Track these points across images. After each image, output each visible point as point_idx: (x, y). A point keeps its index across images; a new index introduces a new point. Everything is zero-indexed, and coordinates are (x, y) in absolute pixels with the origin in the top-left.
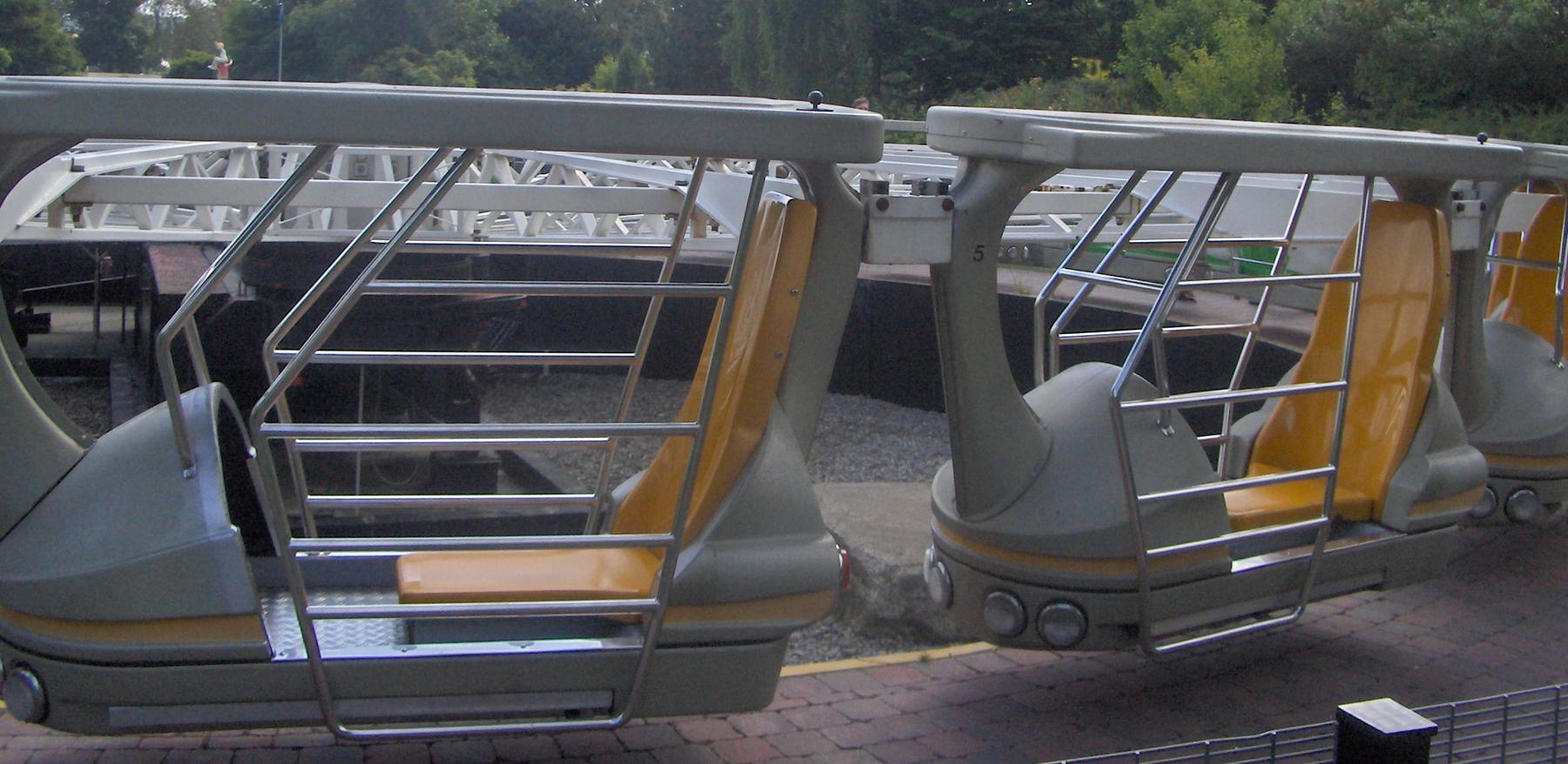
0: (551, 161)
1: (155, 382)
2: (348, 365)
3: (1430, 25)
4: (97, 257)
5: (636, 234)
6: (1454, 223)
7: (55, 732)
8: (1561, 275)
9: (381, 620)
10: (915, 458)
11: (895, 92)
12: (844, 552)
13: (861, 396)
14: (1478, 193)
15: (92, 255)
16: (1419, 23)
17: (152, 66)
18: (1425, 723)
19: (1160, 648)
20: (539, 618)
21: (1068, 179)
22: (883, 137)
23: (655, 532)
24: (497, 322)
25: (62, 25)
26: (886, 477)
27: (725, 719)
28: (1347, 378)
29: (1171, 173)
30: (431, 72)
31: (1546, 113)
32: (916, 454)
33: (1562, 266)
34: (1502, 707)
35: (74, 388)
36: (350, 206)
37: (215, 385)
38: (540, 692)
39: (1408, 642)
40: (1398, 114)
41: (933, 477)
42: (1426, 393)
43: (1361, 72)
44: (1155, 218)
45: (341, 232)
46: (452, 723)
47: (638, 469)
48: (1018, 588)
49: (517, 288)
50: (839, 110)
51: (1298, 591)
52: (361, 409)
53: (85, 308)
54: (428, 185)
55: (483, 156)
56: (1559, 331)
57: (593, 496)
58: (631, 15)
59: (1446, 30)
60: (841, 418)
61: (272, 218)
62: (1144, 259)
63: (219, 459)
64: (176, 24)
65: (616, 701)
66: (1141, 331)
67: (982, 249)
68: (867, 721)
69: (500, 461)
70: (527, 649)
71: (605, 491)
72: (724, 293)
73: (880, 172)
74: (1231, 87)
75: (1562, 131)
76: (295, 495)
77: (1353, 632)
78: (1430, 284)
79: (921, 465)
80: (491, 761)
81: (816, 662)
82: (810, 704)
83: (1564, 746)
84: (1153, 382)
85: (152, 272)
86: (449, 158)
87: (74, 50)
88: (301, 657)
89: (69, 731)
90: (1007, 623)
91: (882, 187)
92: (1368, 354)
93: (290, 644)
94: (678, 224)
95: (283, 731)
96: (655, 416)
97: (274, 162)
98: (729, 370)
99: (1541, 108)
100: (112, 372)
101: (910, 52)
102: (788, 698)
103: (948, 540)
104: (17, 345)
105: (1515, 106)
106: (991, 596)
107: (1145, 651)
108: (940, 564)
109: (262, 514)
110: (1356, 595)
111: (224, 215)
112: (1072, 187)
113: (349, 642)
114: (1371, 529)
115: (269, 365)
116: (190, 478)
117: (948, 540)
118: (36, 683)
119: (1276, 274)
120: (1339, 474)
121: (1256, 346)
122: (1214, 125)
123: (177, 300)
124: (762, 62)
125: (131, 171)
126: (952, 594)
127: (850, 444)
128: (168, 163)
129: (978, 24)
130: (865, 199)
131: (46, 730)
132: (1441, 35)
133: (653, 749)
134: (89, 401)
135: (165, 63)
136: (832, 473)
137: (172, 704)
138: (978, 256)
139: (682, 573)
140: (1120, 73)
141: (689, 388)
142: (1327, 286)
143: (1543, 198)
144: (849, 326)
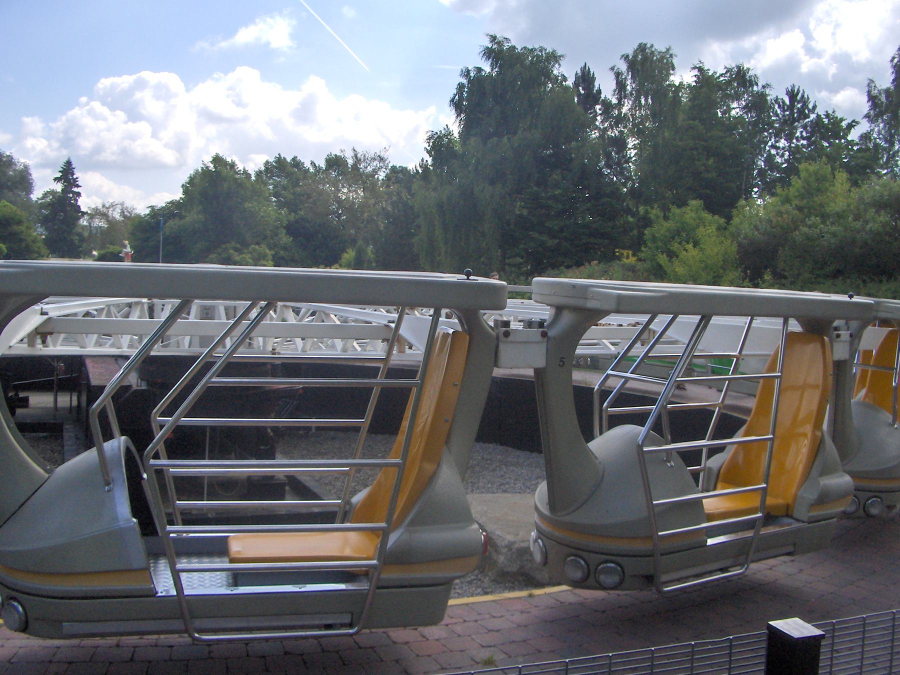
0: (316, 309)
1: (89, 436)
2: (200, 426)
3: (821, 231)
4: (55, 364)
5: (365, 351)
6: (835, 344)
7: (32, 637)
8: (896, 375)
9: (218, 573)
10: (525, 480)
11: (513, 269)
12: (484, 533)
13: (494, 444)
14: (848, 328)
15: (53, 363)
16: (814, 230)
17: (87, 254)
18: (818, 632)
19: (666, 589)
20: (309, 572)
21: (613, 320)
22: (507, 295)
23: (376, 522)
24: (285, 402)
25: (35, 231)
26: (509, 490)
27: (416, 629)
28: (773, 434)
29: (672, 316)
30: (247, 258)
31: (888, 281)
32: (526, 477)
33: (896, 369)
34: (862, 623)
35: (43, 439)
36: (201, 335)
37: (123, 438)
38: (310, 614)
39: (808, 586)
40: (803, 282)
41: (536, 490)
42: (818, 442)
43: (781, 258)
44: (662, 341)
45: (196, 350)
46: (259, 632)
47: (366, 486)
48: (584, 554)
49: (296, 382)
50: (481, 280)
51: (745, 556)
52: (207, 452)
53: (49, 393)
54: (245, 323)
55: (277, 306)
56: (895, 406)
57: (340, 501)
58: (362, 225)
59: (830, 234)
60: (483, 456)
61: (156, 342)
62: (657, 366)
63: (126, 480)
64: (101, 230)
65: (353, 619)
66: (655, 407)
67: (564, 360)
68: (498, 631)
69: (287, 481)
70: (303, 590)
71: (347, 498)
72: (416, 385)
73: (505, 315)
74: (706, 267)
75: (896, 292)
76: (169, 501)
77: (776, 580)
78: (821, 380)
79: (528, 484)
80: (282, 654)
81: (468, 597)
82: (465, 621)
83: (898, 645)
84: (662, 436)
85: (87, 373)
86: (258, 307)
87: (43, 245)
88: (173, 594)
89: (40, 636)
90: (578, 575)
91: (506, 324)
92: (785, 420)
93: (167, 587)
94: (389, 344)
95: (162, 636)
96: (376, 456)
97: (157, 309)
98: (418, 429)
99: (884, 278)
100: (64, 430)
101: (522, 246)
102: (452, 618)
103: (544, 527)
104: (10, 414)
105: (870, 278)
106: (569, 559)
107: (657, 590)
108: (539, 541)
109: (151, 512)
110: (778, 558)
111: (128, 340)
112: (615, 324)
113: (200, 585)
114: (786, 520)
115: (154, 426)
116: (109, 491)
117: (544, 527)
118: (20, 609)
119: (732, 374)
120: (768, 489)
121: (721, 415)
122: (696, 288)
123: (102, 389)
124: (438, 252)
125: (75, 315)
126: (546, 558)
127: (488, 472)
128: (96, 310)
129: (561, 230)
130: (497, 331)
131: (27, 636)
132: (827, 236)
133: (375, 647)
134: (51, 447)
135: (95, 253)
136: (478, 488)
137: (99, 621)
138: (562, 363)
139: (391, 547)
140: (643, 258)
141: (395, 440)
142: (761, 381)
143: (886, 330)
144: (487, 404)
